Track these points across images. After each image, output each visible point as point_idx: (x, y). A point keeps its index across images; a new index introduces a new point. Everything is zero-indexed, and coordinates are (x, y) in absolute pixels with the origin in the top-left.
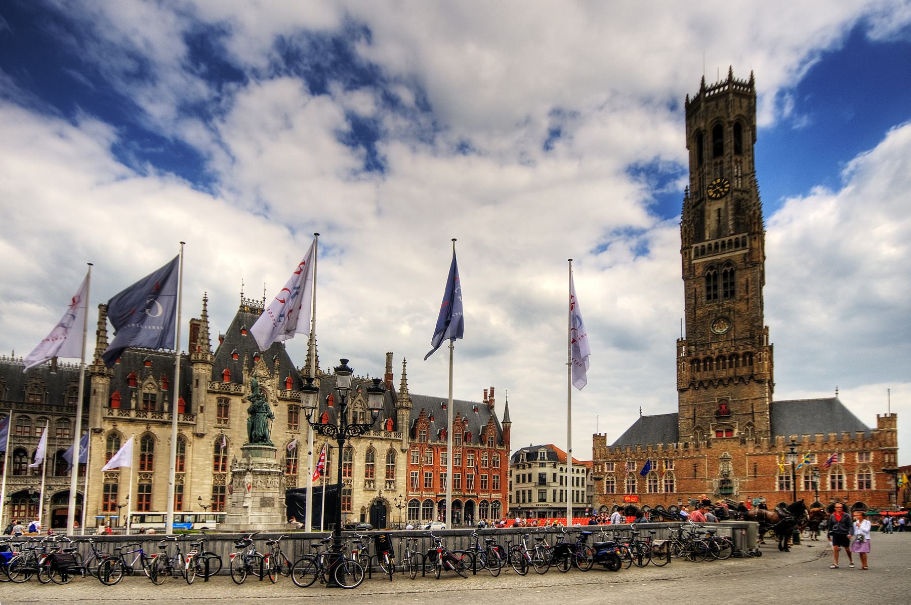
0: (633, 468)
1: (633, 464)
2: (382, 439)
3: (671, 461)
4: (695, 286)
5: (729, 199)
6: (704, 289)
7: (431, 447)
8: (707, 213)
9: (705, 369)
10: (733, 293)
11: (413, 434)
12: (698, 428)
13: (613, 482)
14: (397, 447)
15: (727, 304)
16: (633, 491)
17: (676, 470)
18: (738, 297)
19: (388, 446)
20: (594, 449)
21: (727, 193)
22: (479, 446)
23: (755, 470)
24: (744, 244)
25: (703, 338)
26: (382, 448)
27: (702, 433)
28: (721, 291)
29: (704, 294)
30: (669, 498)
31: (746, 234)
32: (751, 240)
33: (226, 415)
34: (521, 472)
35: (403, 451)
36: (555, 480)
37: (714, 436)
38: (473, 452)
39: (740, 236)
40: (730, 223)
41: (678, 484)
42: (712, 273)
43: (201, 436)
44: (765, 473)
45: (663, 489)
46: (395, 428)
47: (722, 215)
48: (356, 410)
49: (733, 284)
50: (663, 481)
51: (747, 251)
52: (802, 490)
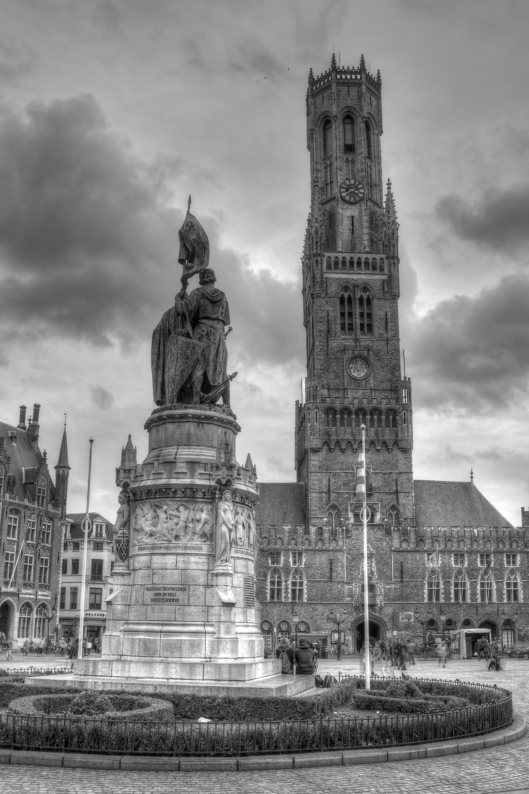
3: (300, 554)
4: (327, 307)
5: (364, 207)
6: (338, 315)
8: (339, 217)
9: (342, 425)
10: (370, 327)
12: (334, 507)
15: (365, 340)
17: (308, 567)
18: (376, 334)
21: (362, 199)
23: (402, 572)
24: (382, 269)
25: (337, 381)
27: (338, 515)
28: (358, 321)
29: (339, 321)
30: (297, 609)
31: (384, 256)
32: (390, 265)
37: (352, 521)
39: (378, 257)
40: (366, 237)
41: (310, 589)
42: (346, 296)
44: (412, 576)
45: (290, 596)
47: (355, 225)
49: (369, 315)
50: (289, 583)
51: (385, 277)
52: (453, 601)
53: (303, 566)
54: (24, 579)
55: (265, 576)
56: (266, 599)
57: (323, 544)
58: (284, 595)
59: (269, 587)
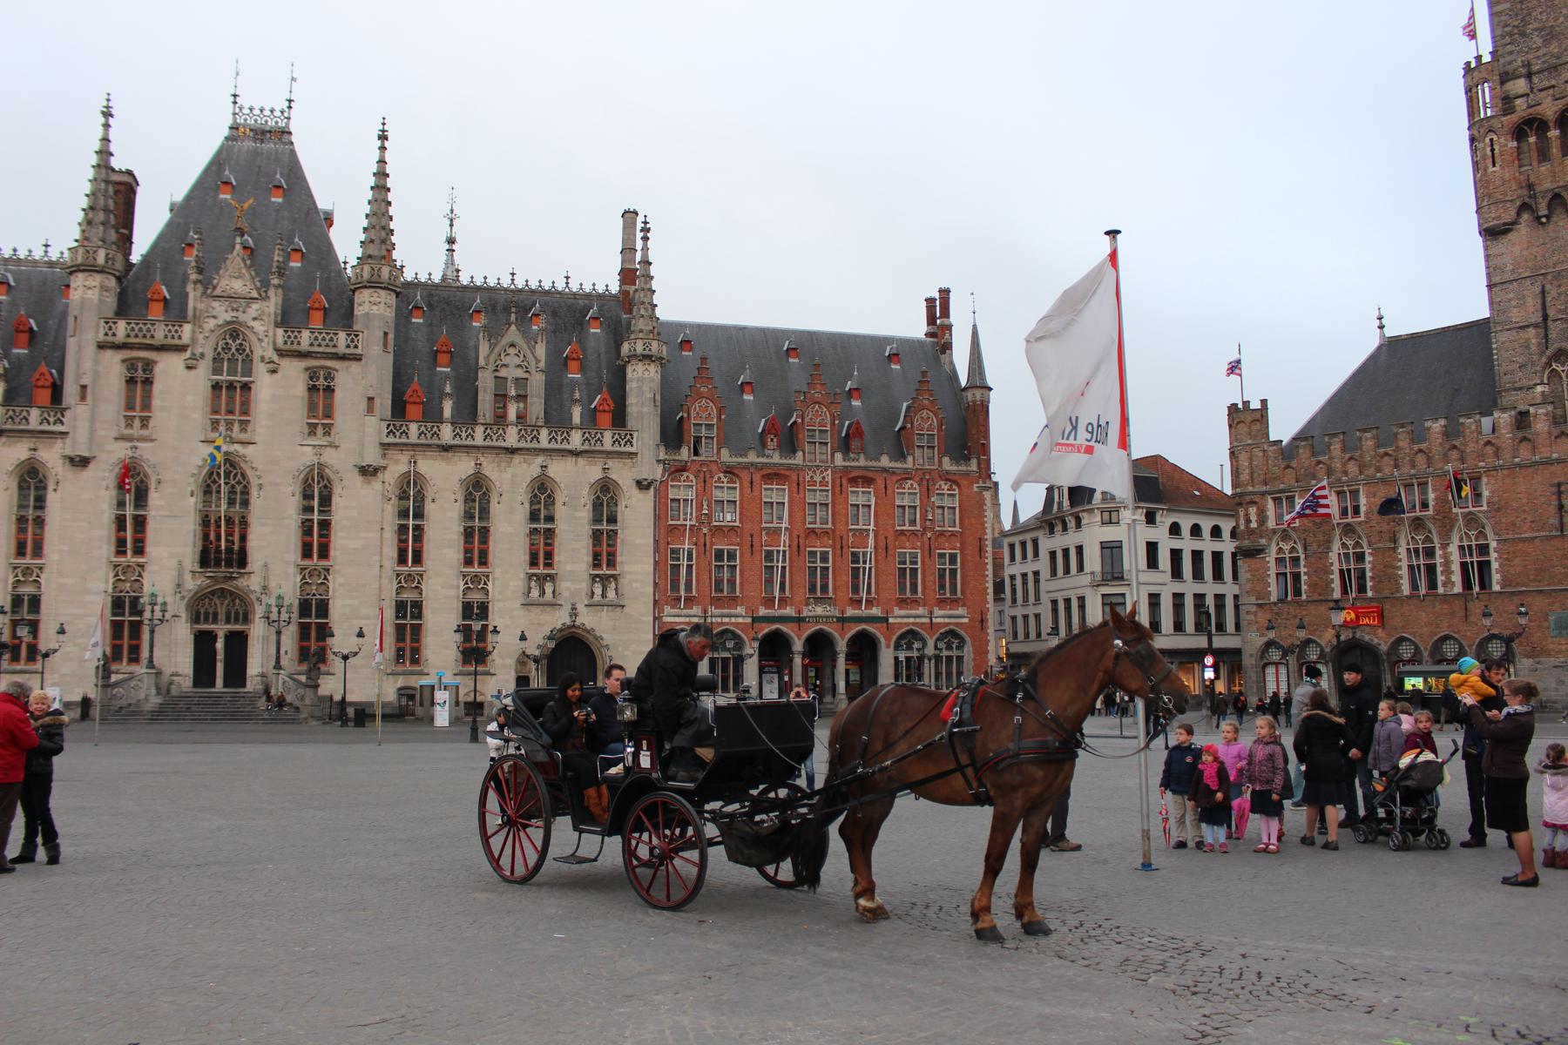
0: (1356, 511)
1: (1355, 494)
2: (575, 454)
7: (730, 471)
11: (673, 433)
13: (1296, 560)
14: (623, 475)
16: (1362, 588)
19: (592, 472)
20: (1232, 454)
22: (885, 461)
26: (574, 480)
33: (147, 406)
34: (1058, 541)
35: (642, 485)
36: (1152, 562)
38: (868, 481)
43: (81, 462)
46: (619, 418)
48: (503, 373)
53: (1485, 508)
54: (902, 589)
55: (1394, 540)
56: (1399, 589)
57: (1534, 451)
58: (1440, 578)
59: (1404, 564)
